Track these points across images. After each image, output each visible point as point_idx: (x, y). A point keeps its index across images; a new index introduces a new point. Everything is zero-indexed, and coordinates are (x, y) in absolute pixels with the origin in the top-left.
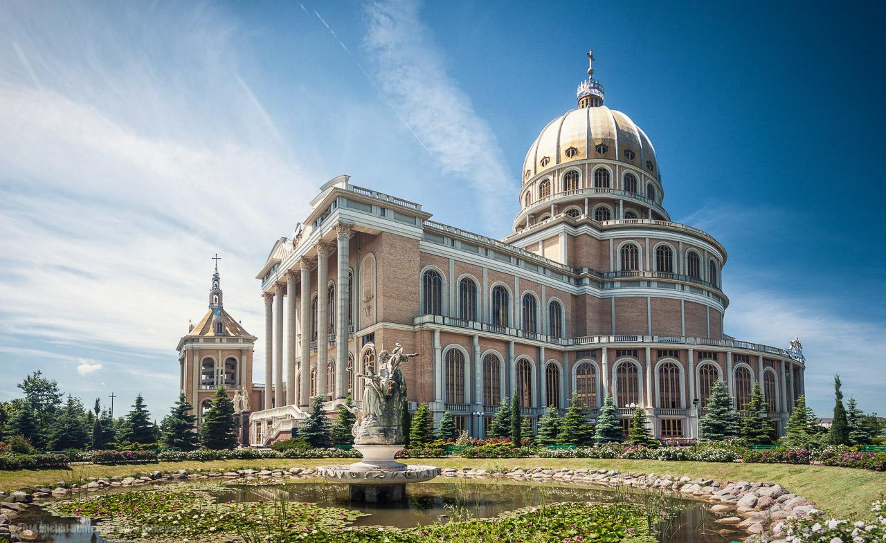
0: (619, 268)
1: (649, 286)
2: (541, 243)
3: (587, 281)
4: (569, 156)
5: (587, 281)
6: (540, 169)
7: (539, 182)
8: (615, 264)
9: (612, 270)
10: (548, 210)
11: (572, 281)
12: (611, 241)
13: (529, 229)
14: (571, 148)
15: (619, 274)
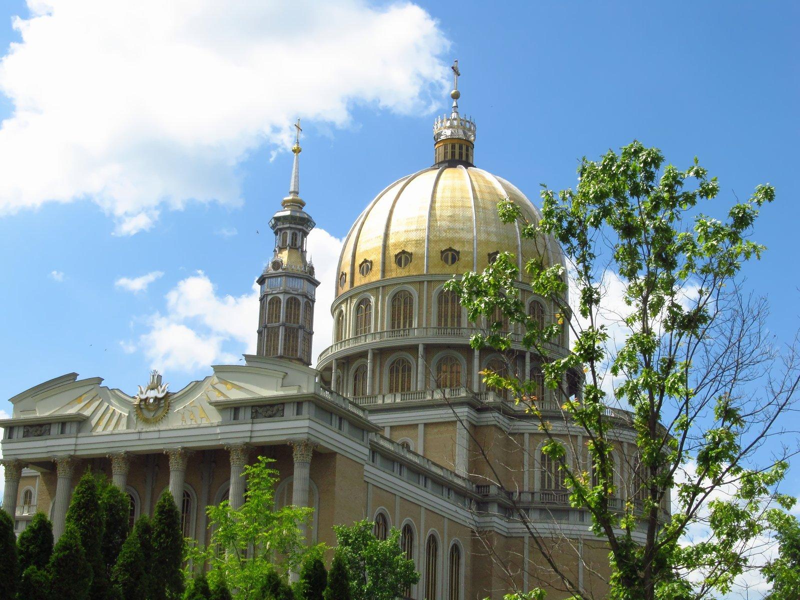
0: (537, 486)
1: (582, 519)
2: (421, 428)
3: (494, 510)
4: (446, 261)
5: (494, 510)
6: (396, 272)
7: (391, 291)
8: (532, 477)
9: (526, 489)
10: (413, 349)
11: (474, 507)
12: (527, 436)
13: (398, 400)
14: (450, 249)
15: (537, 498)
